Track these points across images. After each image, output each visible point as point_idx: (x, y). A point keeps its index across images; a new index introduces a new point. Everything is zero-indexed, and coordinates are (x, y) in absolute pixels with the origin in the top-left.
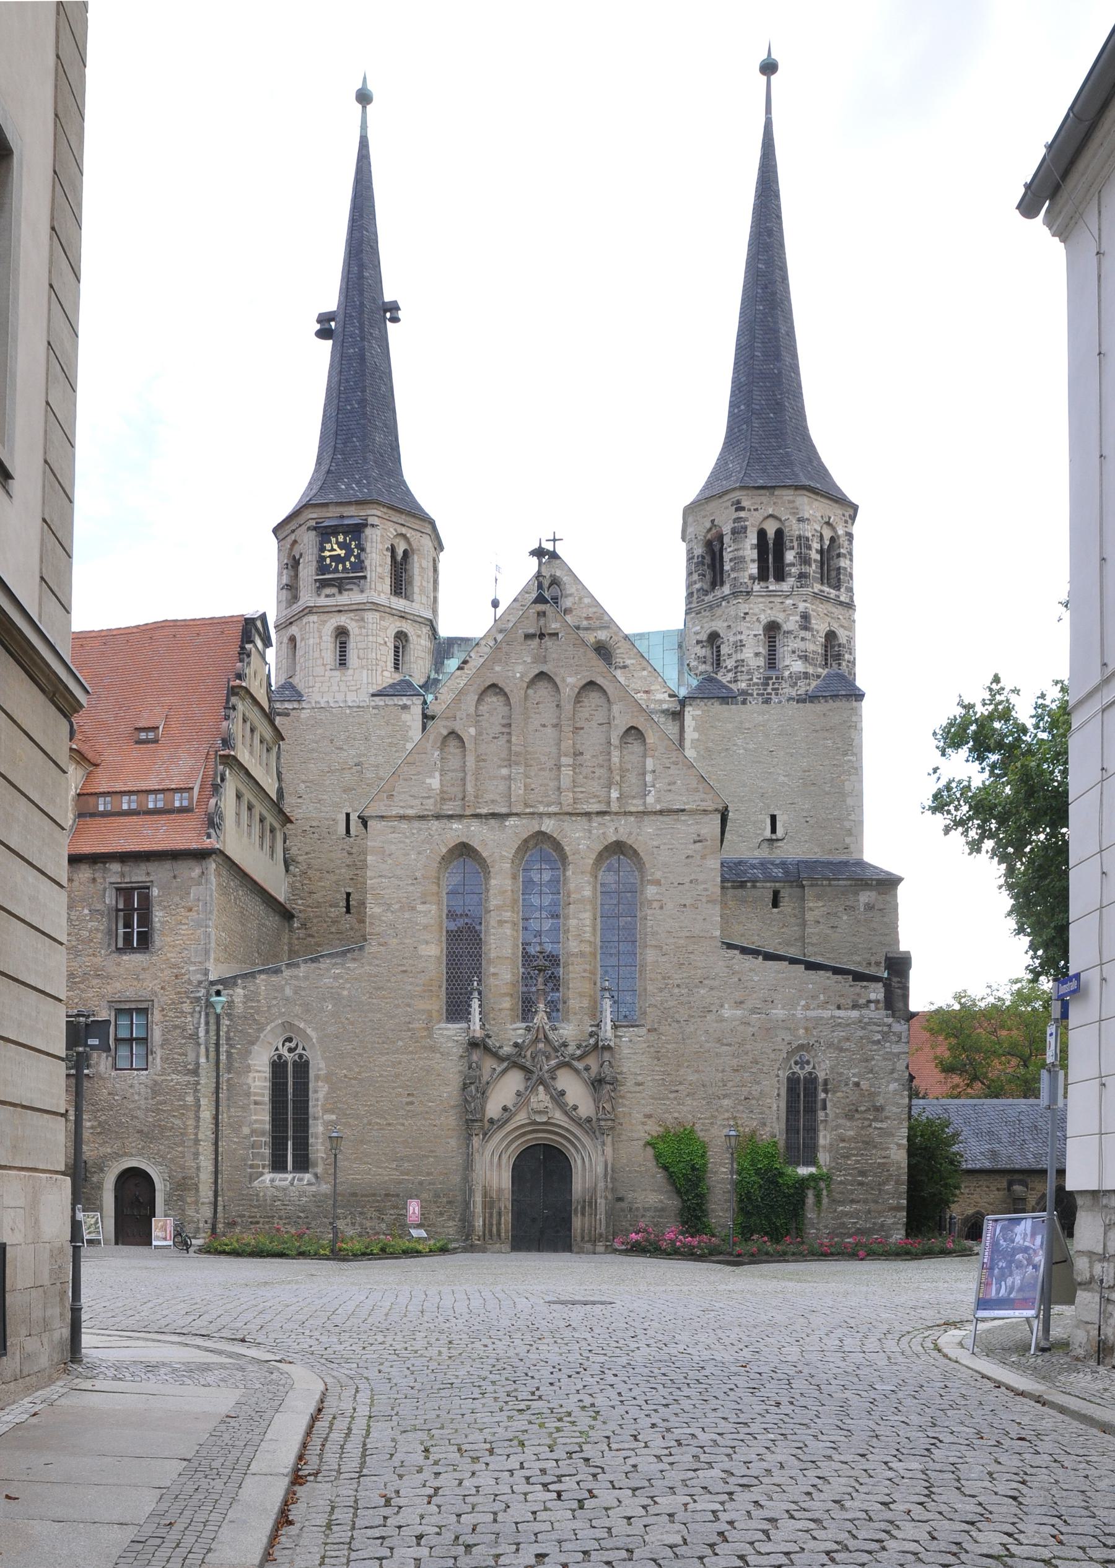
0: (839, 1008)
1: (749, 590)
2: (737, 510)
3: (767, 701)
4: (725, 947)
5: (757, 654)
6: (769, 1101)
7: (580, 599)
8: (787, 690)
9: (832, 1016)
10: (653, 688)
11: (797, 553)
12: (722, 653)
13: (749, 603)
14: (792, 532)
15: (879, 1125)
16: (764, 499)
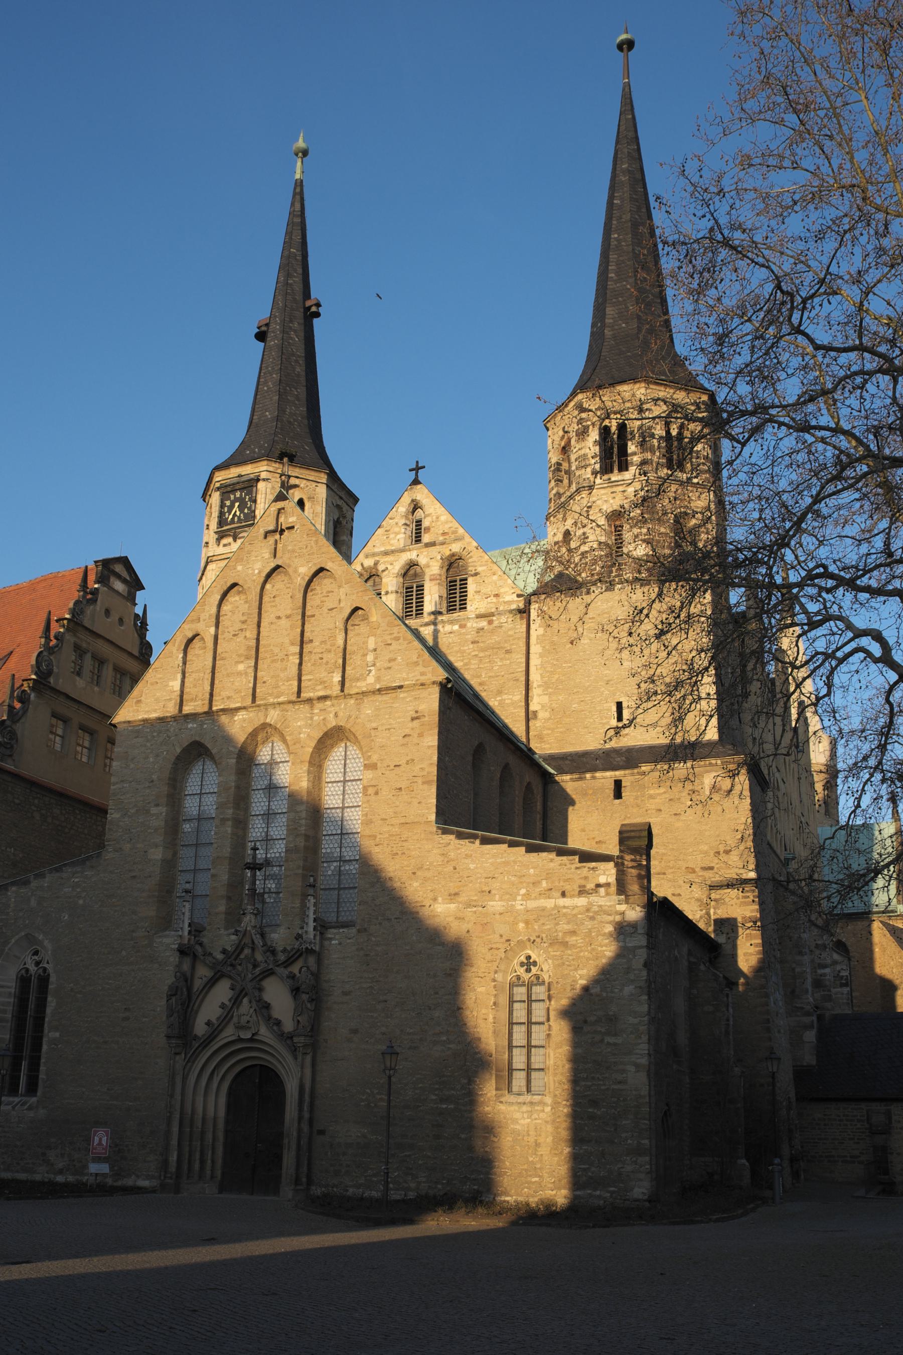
0: (563, 894)
4: (440, 832)
6: (484, 1011)
7: (437, 518)
9: (555, 906)
15: (611, 1040)
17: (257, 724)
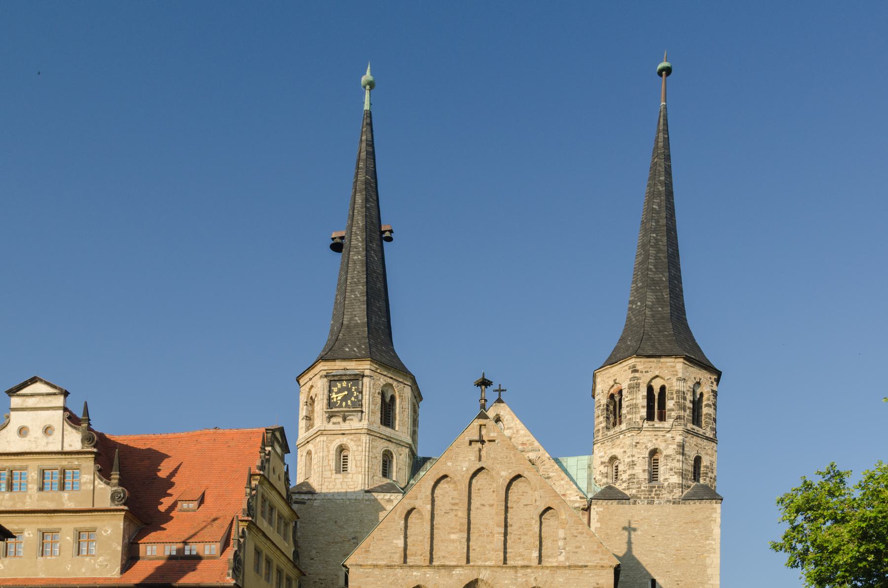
1: (640, 426)
2: (633, 372)
3: (651, 502)
5: (644, 471)
8: (666, 495)
10: (568, 492)
11: (676, 402)
12: (619, 469)
13: (641, 436)
14: (673, 388)
16: (653, 365)
17: (472, 579)
